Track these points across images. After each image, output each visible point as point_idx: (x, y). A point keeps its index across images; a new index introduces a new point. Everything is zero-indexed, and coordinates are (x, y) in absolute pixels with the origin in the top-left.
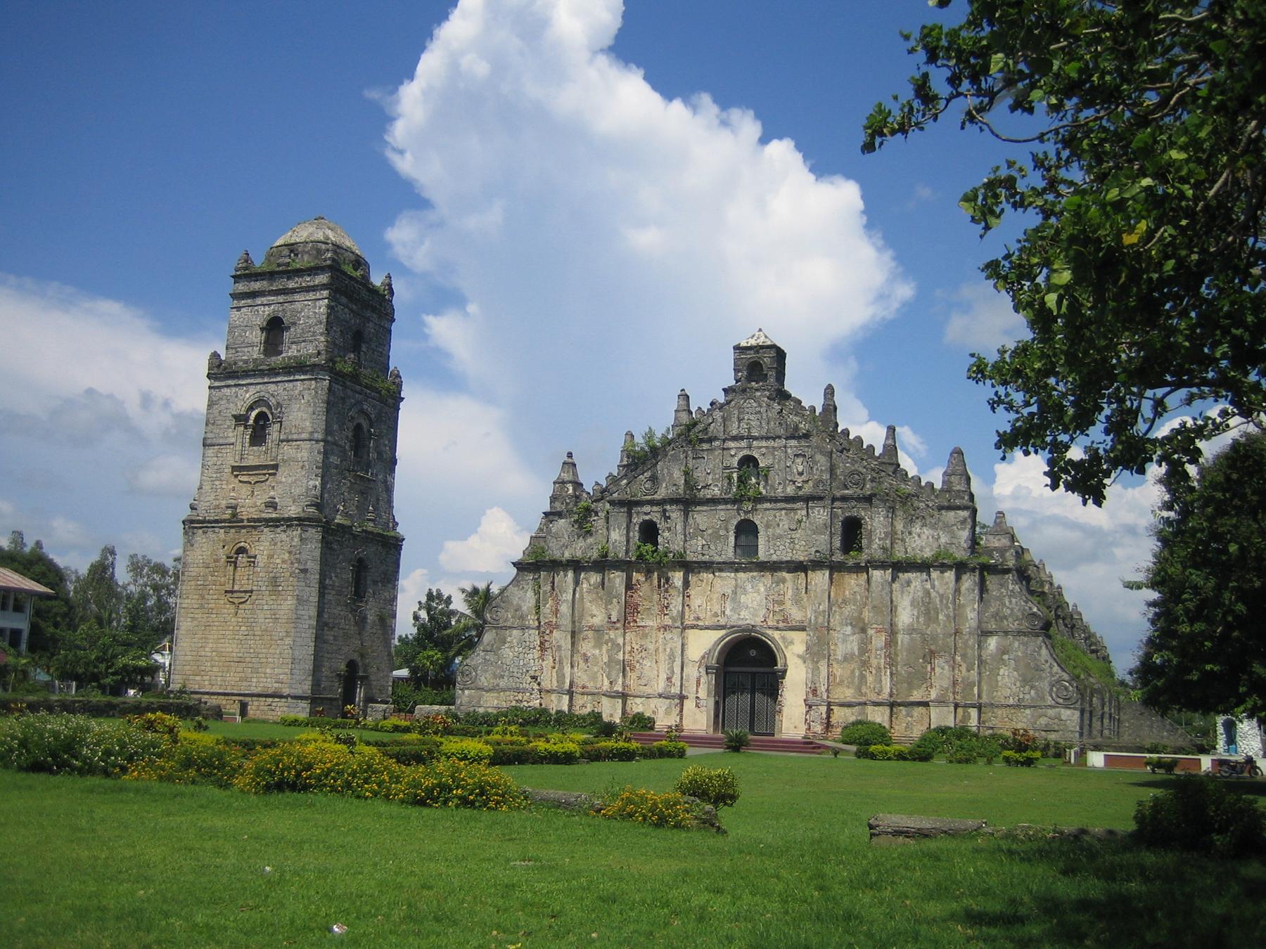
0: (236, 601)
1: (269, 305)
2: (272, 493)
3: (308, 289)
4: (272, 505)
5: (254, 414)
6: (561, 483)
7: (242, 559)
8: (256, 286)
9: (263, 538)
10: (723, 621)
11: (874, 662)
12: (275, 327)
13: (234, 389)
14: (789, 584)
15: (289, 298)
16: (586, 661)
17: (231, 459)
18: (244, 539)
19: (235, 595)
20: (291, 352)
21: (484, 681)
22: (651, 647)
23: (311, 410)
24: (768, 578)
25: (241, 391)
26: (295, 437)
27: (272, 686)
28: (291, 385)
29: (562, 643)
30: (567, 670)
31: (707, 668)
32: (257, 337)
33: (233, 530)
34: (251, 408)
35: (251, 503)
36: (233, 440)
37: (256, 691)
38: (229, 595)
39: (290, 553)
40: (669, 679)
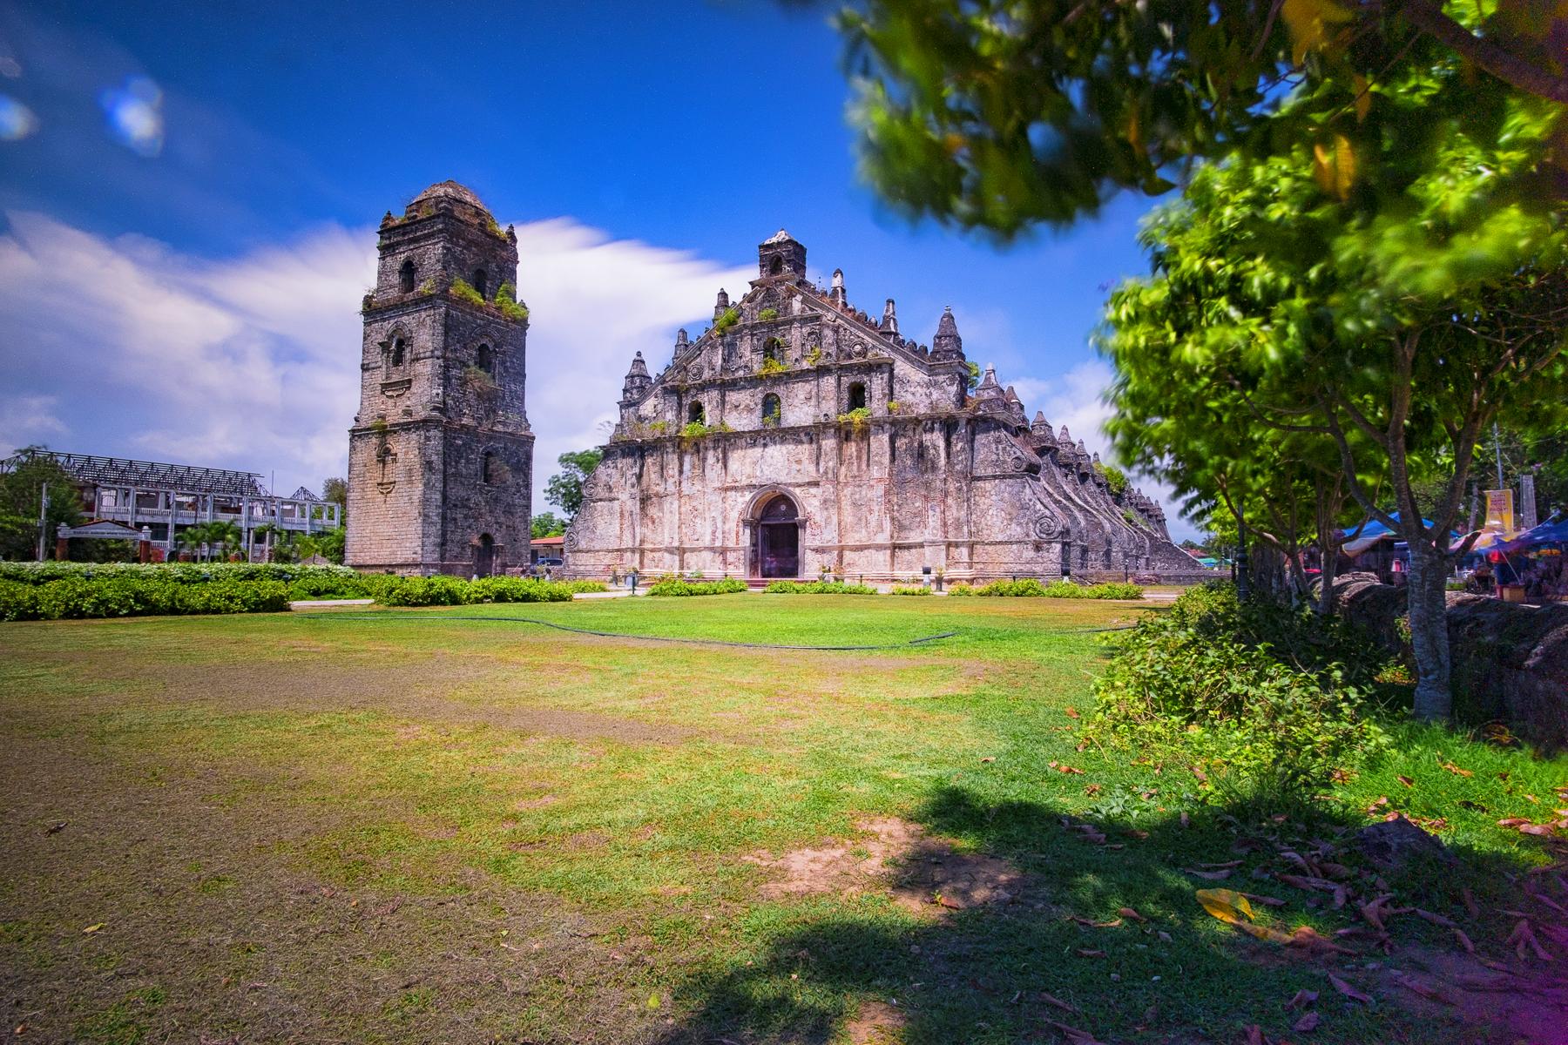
3: (427, 237)
4: (408, 413)
6: (631, 377)
11: (876, 508)
12: (409, 270)
20: (423, 288)
21: (583, 545)
22: (700, 507)
30: (638, 530)
32: (395, 279)
35: (395, 415)
37: (400, 561)
40: (714, 533)
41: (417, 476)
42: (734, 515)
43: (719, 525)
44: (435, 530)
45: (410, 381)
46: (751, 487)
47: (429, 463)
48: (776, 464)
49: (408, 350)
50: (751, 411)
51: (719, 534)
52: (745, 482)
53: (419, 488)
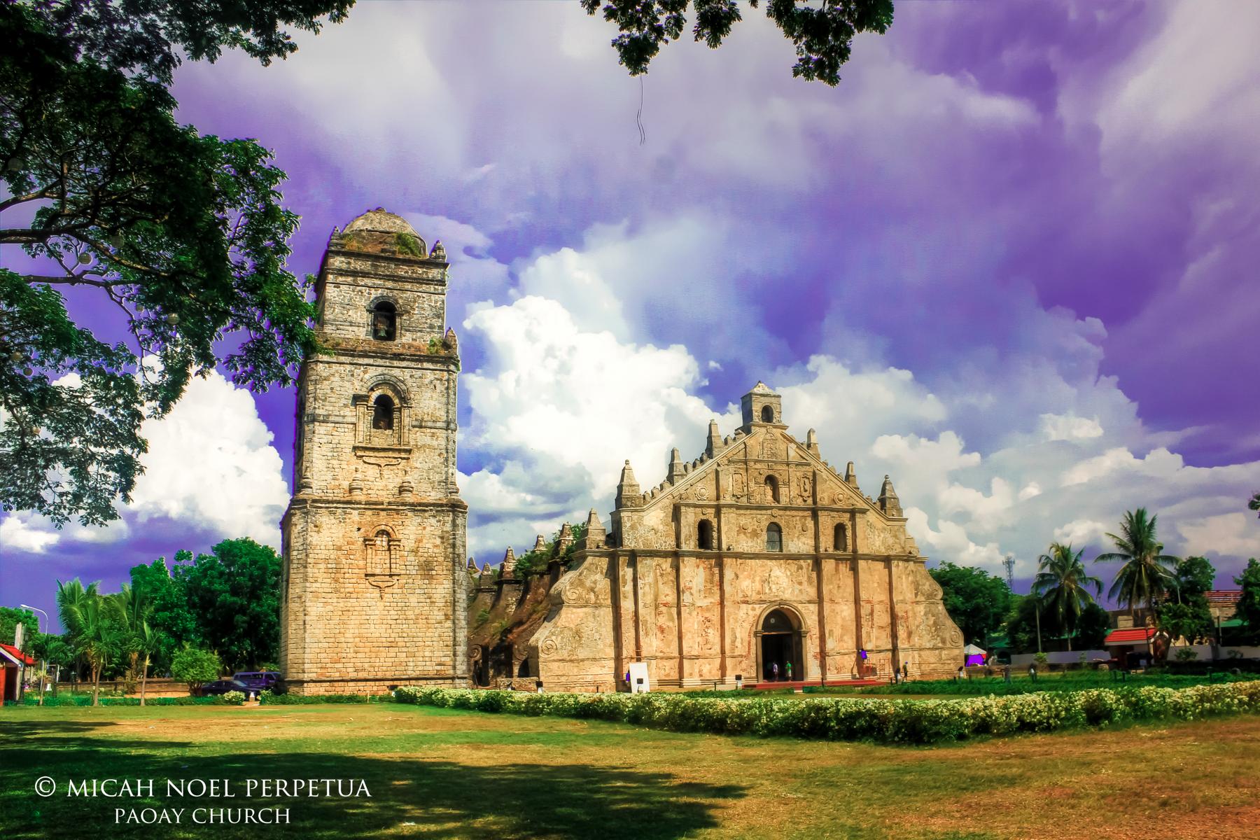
0: (381, 584)
1: (377, 288)
2: (408, 478)
5: (374, 395)
7: (381, 542)
8: (358, 265)
9: (407, 522)
10: (763, 597)
13: (348, 367)
14: (805, 570)
15: (399, 285)
16: (662, 632)
17: (347, 439)
18: (384, 520)
19: (377, 578)
20: (405, 339)
23: (444, 400)
24: (793, 566)
25: (359, 371)
26: (430, 424)
27: (431, 669)
28: (419, 373)
29: (648, 618)
31: (756, 634)
32: (364, 317)
33: (369, 512)
34: (372, 389)
36: (354, 420)
38: (371, 579)
39: (442, 538)
40: (733, 642)
41: (440, 570)
42: (747, 626)
43: (738, 635)
44: (462, 635)
45: (409, 451)
46: (762, 602)
47: (459, 555)
48: (785, 584)
49: (406, 412)
50: (755, 534)
51: (738, 643)
52: (755, 597)
53: (442, 589)
